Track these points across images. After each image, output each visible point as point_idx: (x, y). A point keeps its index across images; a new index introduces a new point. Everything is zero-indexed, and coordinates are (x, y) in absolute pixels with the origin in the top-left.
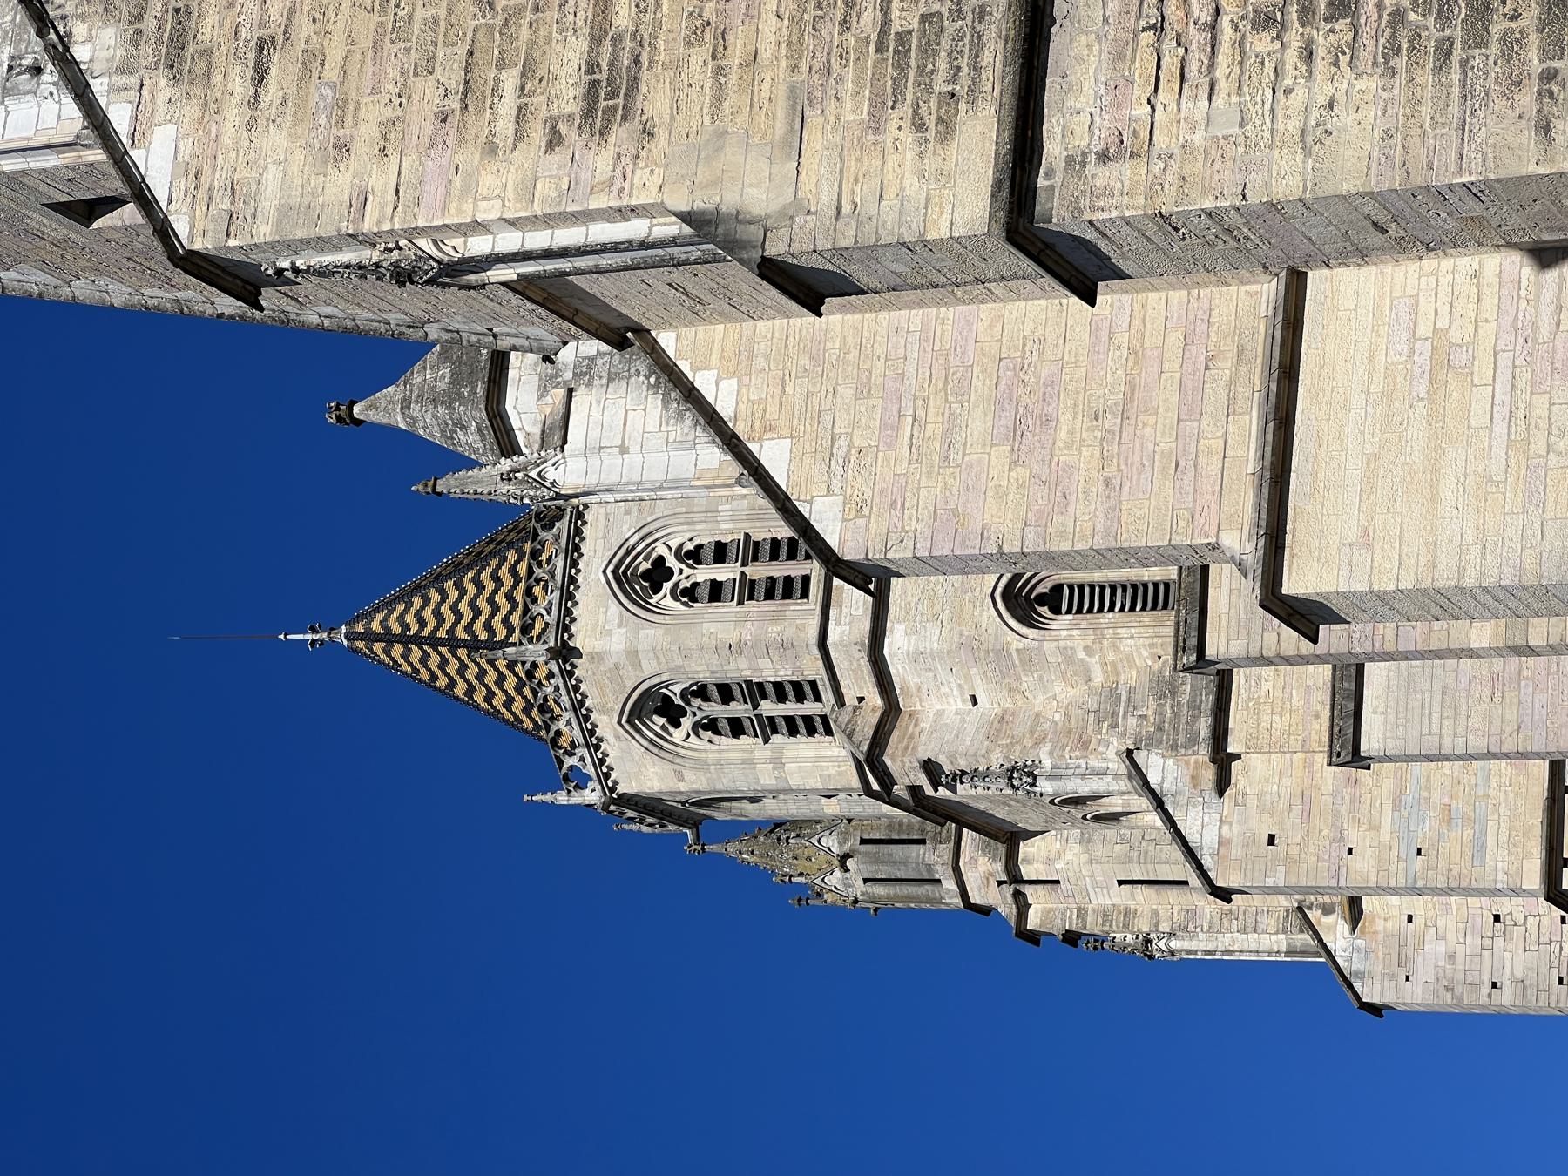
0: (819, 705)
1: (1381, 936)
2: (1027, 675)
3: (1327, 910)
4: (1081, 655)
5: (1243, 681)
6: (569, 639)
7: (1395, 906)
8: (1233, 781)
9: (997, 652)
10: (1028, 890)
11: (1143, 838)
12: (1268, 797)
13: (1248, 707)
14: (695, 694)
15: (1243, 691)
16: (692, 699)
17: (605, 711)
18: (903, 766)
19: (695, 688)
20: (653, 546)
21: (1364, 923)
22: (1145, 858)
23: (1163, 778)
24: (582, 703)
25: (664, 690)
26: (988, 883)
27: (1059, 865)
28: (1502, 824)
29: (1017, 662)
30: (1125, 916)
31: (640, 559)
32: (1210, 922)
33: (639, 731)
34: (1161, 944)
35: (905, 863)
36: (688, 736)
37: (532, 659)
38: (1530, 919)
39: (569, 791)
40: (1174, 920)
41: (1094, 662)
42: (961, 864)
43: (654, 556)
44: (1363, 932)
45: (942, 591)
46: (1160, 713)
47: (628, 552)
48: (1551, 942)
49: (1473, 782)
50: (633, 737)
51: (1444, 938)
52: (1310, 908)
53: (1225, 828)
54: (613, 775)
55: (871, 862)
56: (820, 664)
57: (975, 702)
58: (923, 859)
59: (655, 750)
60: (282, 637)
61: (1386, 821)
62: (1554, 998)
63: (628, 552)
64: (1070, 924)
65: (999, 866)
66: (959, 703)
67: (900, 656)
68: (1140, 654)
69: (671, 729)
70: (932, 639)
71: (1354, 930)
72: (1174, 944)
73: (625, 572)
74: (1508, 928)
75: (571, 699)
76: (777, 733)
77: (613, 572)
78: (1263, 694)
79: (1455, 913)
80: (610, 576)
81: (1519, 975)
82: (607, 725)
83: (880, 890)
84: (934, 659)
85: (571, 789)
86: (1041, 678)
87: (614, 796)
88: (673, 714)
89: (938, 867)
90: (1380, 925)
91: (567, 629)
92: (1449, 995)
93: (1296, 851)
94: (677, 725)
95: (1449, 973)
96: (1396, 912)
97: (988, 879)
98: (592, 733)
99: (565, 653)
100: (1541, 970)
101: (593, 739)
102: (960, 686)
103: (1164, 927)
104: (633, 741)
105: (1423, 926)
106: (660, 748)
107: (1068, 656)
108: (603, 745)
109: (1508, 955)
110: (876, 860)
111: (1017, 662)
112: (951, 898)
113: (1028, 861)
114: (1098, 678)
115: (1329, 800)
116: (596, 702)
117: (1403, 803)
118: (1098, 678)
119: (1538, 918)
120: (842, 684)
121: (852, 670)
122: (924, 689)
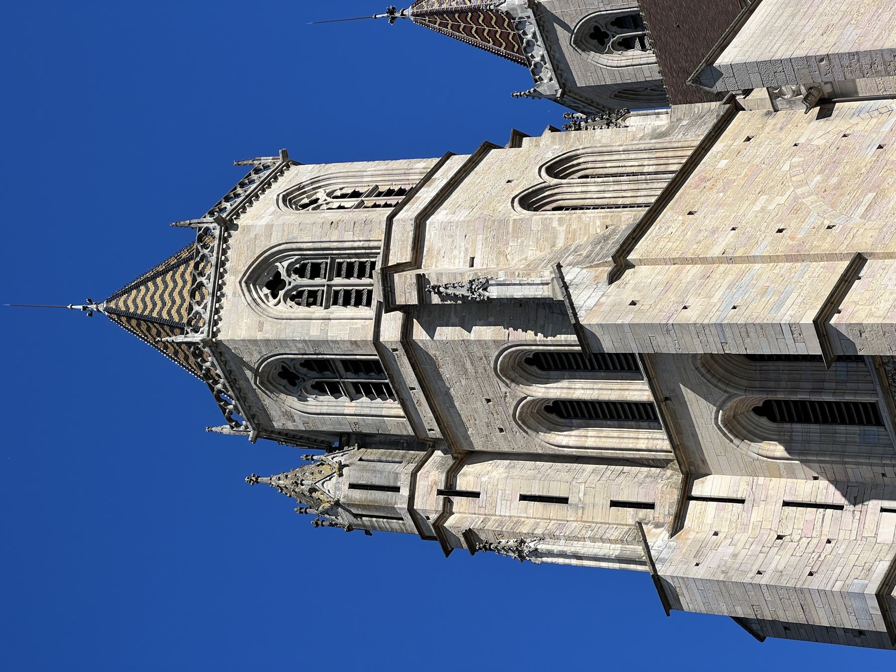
0: (372, 280)
1: (689, 542)
2: (513, 241)
3: (658, 525)
4: (555, 224)
5: (656, 229)
6: (235, 219)
7: (708, 524)
8: (622, 278)
9: (500, 221)
10: (456, 500)
11: (550, 468)
12: (643, 284)
13: (653, 239)
14: (296, 271)
15: (654, 232)
16: (293, 275)
17: (235, 273)
18: (405, 282)
19: (298, 266)
20: (316, 191)
21: (681, 534)
22: (546, 478)
23: (575, 278)
24: (223, 264)
25: (278, 264)
26: (432, 490)
27: (484, 479)
28: (802, 294)
29: (510, 230)
30: (515, 524)
31: (305, 196)
32: (572, 531)
33: (249, 291)
34: (532, 545)
35: (381, 472)
36: (279, 302)
37: (205, 225)
38: (804, 539)
39: (187, 333)
40: (548, 528)
41: (562, 229)
42: (418, 474)
43: (314, 197)
44: (677, 538)
45: (482, 196)
46: (591, 252)
47: (299, 189)
48: (814, 552)
49: (792, 276)
50: (244, 295)
51: (735, 545)
52: (647, 524)
53: (603, 299)
54: (220, 324)
55: (360, 470)
56: (382, 237)
57: (472, 266)
58: (395, 470)
59: (253, 305)
60: (69, 307)
61: (718, 295)
62: (801, 582)
63: (299, 189)
64: (475, 525)
65: (443, 477)
66: (461, 263)
67: (436, 225)
68: (595, 223)
69: (271, 298)
70: (462, 215)
71: (672, 536)
72: (542, 547)
73: (290, 200)
74: (785, 543)
75: (218, 258)
76: (336, 305)
77: (283, 195)
78: (667, 233)
79: (750, 532)
80: (281, 196)
81: (780, 568)
82: (232, 282)
83: (357, 495)
84: (457, 227)
85: (189, 330)
86: (522, 242)
87: (214, 340)
88: (275, 285)
89: (403, 477)
90: (692, 536)
91: (238, 215)
92: (723, 576)
93: (647, 307)
94: (275, 296)
95: (728, 565)
96: (707, 528)
97: (432, 487)
98: (220, 288)
99: (229, 225)
100: (798, 567)
101: (219, 292)
102: (466, 249)
103: (539, 531)
104: (243, 297)
105: (722, 538)
106: (258, 304)
107: (546, 227)
108: (223, 300)
109: (778, 557)
110: (364, 469)
111: (510, 230)
112: (401, 503)
113: (464, 475)
114: (560, 244)
115: (684, 285)
116: (232, 264)
117: (736, 286)
118: (560, 244)
119: (810, 539)
120: (391, 252)
121: (402, 241)
122: (442, 253)
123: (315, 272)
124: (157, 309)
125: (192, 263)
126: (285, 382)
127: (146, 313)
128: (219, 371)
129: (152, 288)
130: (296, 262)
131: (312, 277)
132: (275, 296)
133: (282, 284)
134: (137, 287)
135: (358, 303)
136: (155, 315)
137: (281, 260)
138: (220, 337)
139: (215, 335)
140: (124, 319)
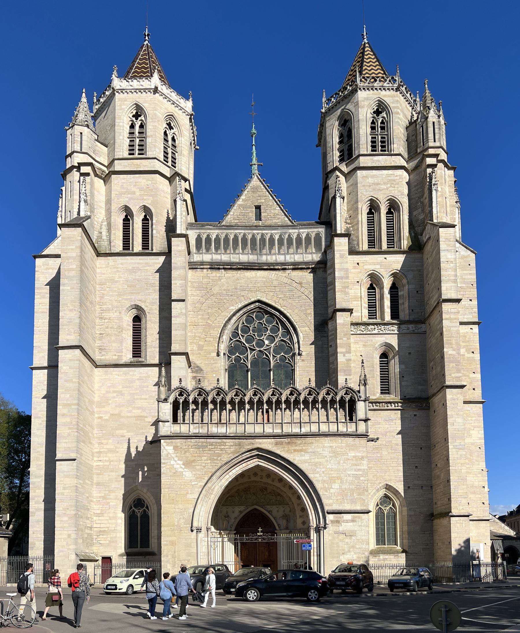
14: (382, 120)
69: (373, 111)
88: (377, 112)
123: (382, 128)
124: (367, 64)
125: (384, 76)
126: (343, 122)
127: (365, 60)
128: (346, 93)
129: (374, 61)
130: (386, 120)
131: (380, 127)
132: (374, 112)
133: (378, 115)
134: (374, 54)
135: (372, 146)
136: (365, 63)
137: (386, 113)
138: (359, 91)
139: (360, 89)
140: (362, 51)
